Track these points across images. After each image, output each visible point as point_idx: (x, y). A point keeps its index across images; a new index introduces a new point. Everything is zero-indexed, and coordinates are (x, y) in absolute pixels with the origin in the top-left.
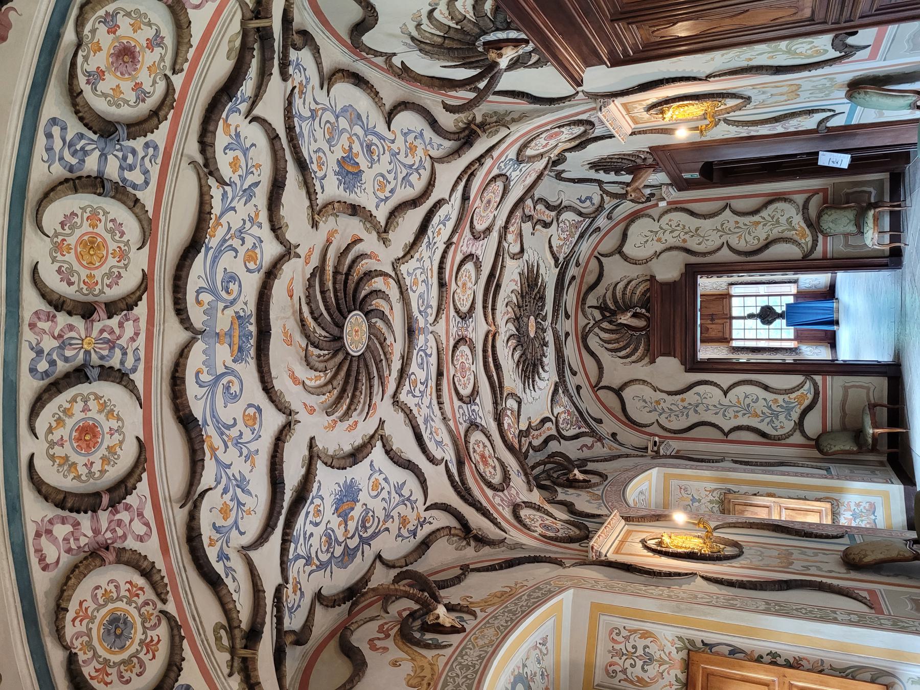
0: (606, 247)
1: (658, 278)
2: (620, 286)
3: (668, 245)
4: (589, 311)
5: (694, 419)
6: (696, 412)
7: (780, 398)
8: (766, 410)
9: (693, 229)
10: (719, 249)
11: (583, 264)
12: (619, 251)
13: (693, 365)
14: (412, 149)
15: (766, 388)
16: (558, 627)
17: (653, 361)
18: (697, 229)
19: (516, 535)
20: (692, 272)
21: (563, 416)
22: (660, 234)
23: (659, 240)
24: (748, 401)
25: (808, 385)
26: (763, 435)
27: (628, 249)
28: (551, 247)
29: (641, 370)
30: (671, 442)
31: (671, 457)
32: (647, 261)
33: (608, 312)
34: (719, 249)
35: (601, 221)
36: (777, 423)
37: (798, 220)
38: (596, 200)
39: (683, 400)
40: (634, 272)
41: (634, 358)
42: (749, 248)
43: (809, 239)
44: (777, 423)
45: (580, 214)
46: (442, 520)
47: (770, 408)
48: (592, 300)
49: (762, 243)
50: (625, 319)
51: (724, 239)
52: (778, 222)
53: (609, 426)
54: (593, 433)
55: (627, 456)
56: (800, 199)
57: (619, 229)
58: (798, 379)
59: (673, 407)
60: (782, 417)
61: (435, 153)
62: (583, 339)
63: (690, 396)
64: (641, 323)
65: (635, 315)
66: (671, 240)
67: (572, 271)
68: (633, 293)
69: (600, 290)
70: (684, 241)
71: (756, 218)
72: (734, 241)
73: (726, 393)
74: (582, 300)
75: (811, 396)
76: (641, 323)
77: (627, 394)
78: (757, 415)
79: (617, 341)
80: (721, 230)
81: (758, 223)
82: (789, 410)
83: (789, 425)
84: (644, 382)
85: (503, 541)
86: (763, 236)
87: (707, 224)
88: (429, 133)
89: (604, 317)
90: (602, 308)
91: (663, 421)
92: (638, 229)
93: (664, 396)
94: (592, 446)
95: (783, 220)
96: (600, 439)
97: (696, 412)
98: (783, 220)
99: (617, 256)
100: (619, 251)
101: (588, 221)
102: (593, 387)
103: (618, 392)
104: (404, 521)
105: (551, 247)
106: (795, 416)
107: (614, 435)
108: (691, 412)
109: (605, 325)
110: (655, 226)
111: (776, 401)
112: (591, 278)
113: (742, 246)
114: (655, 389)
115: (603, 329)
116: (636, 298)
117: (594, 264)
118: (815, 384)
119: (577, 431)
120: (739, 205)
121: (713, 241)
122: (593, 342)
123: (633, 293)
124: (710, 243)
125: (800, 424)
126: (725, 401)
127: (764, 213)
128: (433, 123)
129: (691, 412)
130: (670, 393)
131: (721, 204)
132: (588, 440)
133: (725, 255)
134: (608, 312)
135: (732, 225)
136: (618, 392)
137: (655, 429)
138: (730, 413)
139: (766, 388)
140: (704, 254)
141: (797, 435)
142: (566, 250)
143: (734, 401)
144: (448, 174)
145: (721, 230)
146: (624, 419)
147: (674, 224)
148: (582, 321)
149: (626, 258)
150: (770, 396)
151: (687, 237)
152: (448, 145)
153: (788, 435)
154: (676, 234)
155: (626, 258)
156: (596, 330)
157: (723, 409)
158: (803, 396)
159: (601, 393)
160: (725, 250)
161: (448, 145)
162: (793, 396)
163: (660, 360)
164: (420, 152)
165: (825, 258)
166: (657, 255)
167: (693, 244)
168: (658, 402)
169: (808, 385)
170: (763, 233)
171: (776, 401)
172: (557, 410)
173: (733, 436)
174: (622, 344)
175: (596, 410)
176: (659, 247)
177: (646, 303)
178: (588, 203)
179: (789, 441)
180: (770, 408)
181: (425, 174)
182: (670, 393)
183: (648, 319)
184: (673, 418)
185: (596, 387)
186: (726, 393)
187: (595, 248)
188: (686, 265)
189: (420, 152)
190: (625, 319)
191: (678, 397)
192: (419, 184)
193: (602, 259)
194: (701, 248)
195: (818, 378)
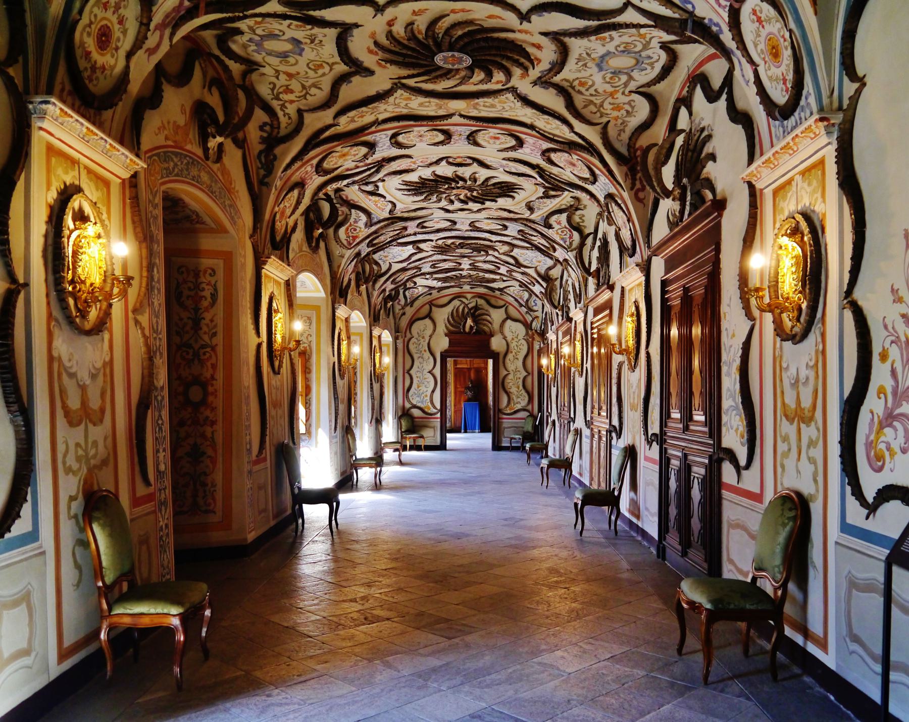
0: (511, 309)
1: (493, 338)
2: (488, 318)
3: (510, 344)
4: (474, 300)
5: (415, 356)
6: (419, 357)
7: (428, 398)
8: (421, 391)
9: (518, 357)
10: (506, 370)
11: (502, 297)
12: (509, 317)
13: (444, 356)
14: (539, 262)
15: (433, 391)
16: (356, 322)
17: (446, 335)
18: (517, 359)
19: (376, 293)
20: (495, 356)
21: (416, 291)
22: (516, 340)
23: (513, 339)
24: (426, 383)
25: (435, 411)
26: (409, 390)
27: (509, 321)
28: (509, 287)
29: (441, 329)
30: (402, 344)
31: (396, 345)
32: (502, 333)
33: (476, 313)
34: (506, 370)
35: (523, 310)
36: (415, 397)
37: (519, 407)
38: (535, 308)
39: (425, 351)
40: (496, 326)
41: (448, 325)
42: (506, 384)
43: (509, 412)
44: (415, 397)
45: (527, 301)
46: (384, 268)
47: (423, 393)
48: (481, 302)
49: (508, 390)
50: (469, 322)
51: (511, 372)
52: (518, 397)
53: (410, 311)
54: (406, 305)
55: (395, 323)
56: (530, 407)
57: (520, 317)
58: (438, 406)
59: (421, 346)
60: (418, 399)
61: (538, 268)
62: (457, 296)
63: (427, 354)
64: (467, 329)
65: (471, 327)
66: (513, 345)
67: (498, 293)
68: (485, 325)
69: (486, 307)
70: (512, 352)
71: (521, 387)
72: (511, 377)
73: (429, 372)
74: (480, 296)
75: (429, 411)
76: (467, 329)
77: (427, 321)
78: (418, 387)
79: (458, 316)
80: (516, 371)
81: (518, 388)
82: (422, 402)
83: (414, 402)
84: (434, 330)
85: (374, 289)
86: (511, 390)
87: (520, 363)
88: (546, 267)
89: (470, 309)
90: (476, 308)
91: (413, 340)
92: (520, 329)
93: (427, 341)
94: (399, 304)
95: (519, 400)
96: (403, 308)
97: (419, 357)
98: (519, 400)
99: (505, 316)
100: (509, 317)
101: (524, 304)
102: (431, 302)
103: (429, 316)
104: (386, 257)
105: (509, 287)
106: (419, 405)
107: (404, 314)
108: (419, 355)
109: (466, 310)
110: (521, 336)
111: (426, 396)
112: (493, 301)
113: (507, 381)
114: (431, 336)
115: (464, 308)
116: (481, 326)
117: (502, 303)
118: (437, 413)
119: (408, 297)
120: (529, 379)
121: (511, 366)
122: (456, 303)
123: (485, 325)
124: (509, 365)
125: (415, 407)
126: (425, 372)
127: (523, 391)
128: (550, 269)
129: (419, 355)
130: (429, 344)
131: (530, 370)
132: (403, 302)
133: (503, 373)
134: (476, 313)
135: (518, 376)
136: (429, 316)
137: (408, 335)
138: (419, 374)
139: (433, 391)
140: (504, 363)
141: (410, 406)
142: (508, 292)
143: (425, 376)
144: (531, 272)
145: (516, 371)
146: (414, 319)
147: (521, 347)
148: (469, 296)
149: (504, 321)
150: (429, 393)
151: (514, 353)
152: (543, 272)
153: (409, 401)
154: (516, 348)
155: (504, 321)
156: (463, 305)
157: (421, 371)
158: (429, 408)
159: (427, 307)
160: (506, 373)
161: (543, 272)
162: (429, 404)
163: (447, 339)
164: (538, 264)
165: (499, 418)
166: (505, 338)
167: (510, 356)
168: (423, 338)
169: (435, 411)
170: (513, 390)
171: (426, 396)
172: (420, 288)
173: (407, 376)
174: (456, 318)
175: (417, 304)
176: (509, 339)
177: (479, 332)
178: (533, 304)
179: (406, 401)
180: (423, 393)
181: (529, 265)
182: (429, 344)
183: (469, 333)
184: (415, 345)
185: (431, 304)
186: (429, 372)
187: (510, 304)
188: (498, 354)
189: (538, 264)
190: (469, 322)
191: (427, 349)
192: (525, 263)
193: (504, 308)
194: (507, 361)
195: (439, 415)
